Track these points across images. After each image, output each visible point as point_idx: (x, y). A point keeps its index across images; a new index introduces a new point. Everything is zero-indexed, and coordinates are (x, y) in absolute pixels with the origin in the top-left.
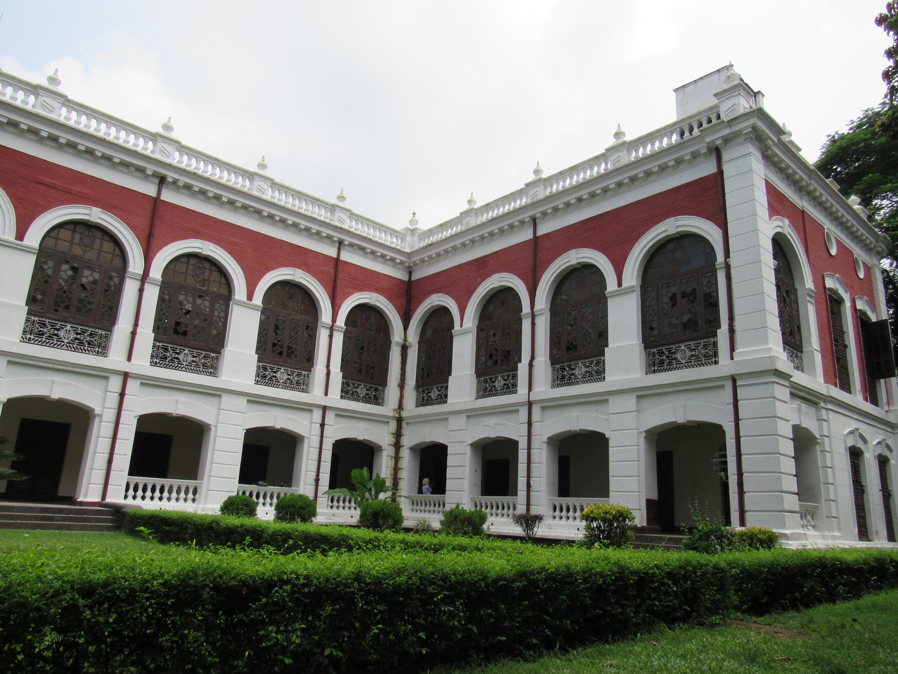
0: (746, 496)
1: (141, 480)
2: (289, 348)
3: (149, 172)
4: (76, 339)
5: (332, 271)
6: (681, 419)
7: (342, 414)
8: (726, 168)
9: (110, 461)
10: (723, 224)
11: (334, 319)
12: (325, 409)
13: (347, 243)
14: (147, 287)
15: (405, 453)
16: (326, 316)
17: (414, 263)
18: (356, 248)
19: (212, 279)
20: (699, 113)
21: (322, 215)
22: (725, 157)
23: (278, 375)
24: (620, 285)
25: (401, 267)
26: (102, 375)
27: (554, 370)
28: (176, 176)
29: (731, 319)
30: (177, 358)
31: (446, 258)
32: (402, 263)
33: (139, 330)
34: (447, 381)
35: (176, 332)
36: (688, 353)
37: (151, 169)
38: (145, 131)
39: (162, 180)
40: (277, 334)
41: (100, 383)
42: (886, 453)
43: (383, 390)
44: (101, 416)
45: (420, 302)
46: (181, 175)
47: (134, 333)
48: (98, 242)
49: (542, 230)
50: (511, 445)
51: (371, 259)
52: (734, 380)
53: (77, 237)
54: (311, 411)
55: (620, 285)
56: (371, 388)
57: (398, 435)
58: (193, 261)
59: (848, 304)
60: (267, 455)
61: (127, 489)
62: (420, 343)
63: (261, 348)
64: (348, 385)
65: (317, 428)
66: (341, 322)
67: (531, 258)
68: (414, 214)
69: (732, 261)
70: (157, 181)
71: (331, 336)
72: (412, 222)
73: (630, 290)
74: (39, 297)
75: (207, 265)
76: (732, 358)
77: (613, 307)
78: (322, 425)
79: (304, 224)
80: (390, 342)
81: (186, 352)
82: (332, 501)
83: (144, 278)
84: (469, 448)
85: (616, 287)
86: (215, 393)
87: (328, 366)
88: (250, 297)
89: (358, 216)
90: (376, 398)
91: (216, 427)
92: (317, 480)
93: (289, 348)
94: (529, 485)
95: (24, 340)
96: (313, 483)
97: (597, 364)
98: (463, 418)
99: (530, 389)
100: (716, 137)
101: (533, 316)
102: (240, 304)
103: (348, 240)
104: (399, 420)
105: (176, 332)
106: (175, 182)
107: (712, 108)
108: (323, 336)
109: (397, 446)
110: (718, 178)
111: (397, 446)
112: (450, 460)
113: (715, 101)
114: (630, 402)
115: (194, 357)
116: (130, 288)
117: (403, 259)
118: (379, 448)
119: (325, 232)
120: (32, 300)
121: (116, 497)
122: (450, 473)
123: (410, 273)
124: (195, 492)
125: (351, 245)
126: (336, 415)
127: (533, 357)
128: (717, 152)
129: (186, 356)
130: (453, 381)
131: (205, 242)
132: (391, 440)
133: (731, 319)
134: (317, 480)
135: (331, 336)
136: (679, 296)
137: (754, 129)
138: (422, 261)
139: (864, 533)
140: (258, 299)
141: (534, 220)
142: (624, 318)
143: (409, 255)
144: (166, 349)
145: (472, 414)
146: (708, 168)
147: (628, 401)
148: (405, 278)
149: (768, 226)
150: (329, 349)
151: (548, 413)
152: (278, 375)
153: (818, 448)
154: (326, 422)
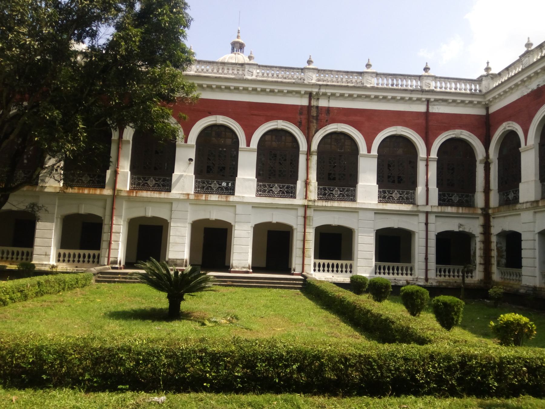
1: (322, 261)
2: (399, 177)
3: (303, 93)
4: (281, 191)
5: (424, 122)
9: (304, 253)
11: (428, 153)
12: (427, 213)
13: (432, 100)
15: (494, 239)
16: (422, 152)
17: (489, 100)
18: (441, 102)
19: (346, 143)
21: (413, 84)
23: (393, 195)
25: (480, 106)
28: (317, 90)
30: (332, 193)
31: (512, 93)
32: (479, 103)
34: (518, 187)
35: (329, 179)
37: (303, 90)
38: (298, 69)
39: (310, 95)
40: (390, 170)
41: (293, 212)
43: (473, 196)
44: (296, 229)
45: (496, 129)
48: (283, 138)
51: (455, 106)
53: (274, 137)
54: (418, 215)
56: (462, 195)
57: (487, 227)
58: (334, 136)
60: (393, 246)
62: (499, 159)
63: (380, 181)
64: (444, 195)
65: (423, 226)
66: (434, 155)
68: (488, 63)
70: (308, 96)
71: (427, 166)
72: (487, 69)
74: (261, 172)
75: (342, 137)
78: (427, 224)
79: (399, 95)
80: (476, 161)
81: (336, 189)
82: (440, 272)
84: (537, 236)
86: (355, 211)
87: (427, 185)
88: (369, 151)
89: (441, 78)
92: (426, 259)
93: (399, 177)
96: (424, 260)
102: (364, 156)
103: (432, 97)
105: (329, 179)
106: (317, 94)
108: (421, 166)
112: (524, 245)
115: (341, 191)
116: (302, 159)
117: (480, 100)
119: (415, 96)
120: (258, 175)
122: (524, 253)
124: (351, 267)
125: (436, 100)
126: (436, 216)
129: (336, 192)
130: (522, 186)
131: (339, 124)
134: (426, 259)
135: (427, 166)
138: (495, 98)
140: (374, 151)
143: (484, 95)
144: (325, 189)
148: (482, 112)
150: (427, 175)
152: (393, 195)
154: (429, 222)
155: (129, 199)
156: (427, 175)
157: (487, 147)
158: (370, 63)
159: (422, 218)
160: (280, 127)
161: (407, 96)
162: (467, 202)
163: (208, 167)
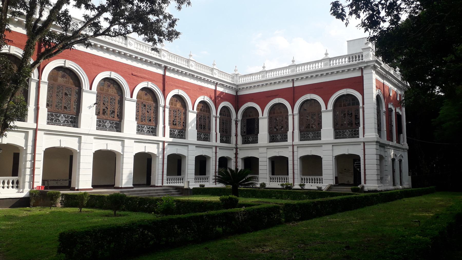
0: (366, 176)
1: (171, 177)
6: (347, 153)
7: (221, 148)
8: (364, 76)
10: (362, 94)
11: (217, 114)
12: (216, 147)
14: (166, 109)
17: (240, 89)
20: (356, 54)
22: (365, 72)
24: (326, 109)
26: (157, 142)
27: (301, 134)
29: (364, 124)
33: (166, 125)
36: (349, 133)
37: (163, 65)
39: (166, 68)
42: (402, 158)
46: (172, 65)
47: (164, 127)
49: (297, 84)
50: (285, 160)
52: (364, 143)
55: (326, 109)
57: (236, 154)
59: (394, 111)
61: (167, 180)
65: (214, 154)
67: (292, 94)
69: (365, 106)
71: (216, 120)
73: (329, 111)
76: (364, 137)
77: (324, 115)
78: (216, 153)
83: (164, 107)
85: (325, 109)
86: (186, 145)
87: (216, 131)
88: (193, 109)
90: (228, 141)
91: (188, 157)
94: (293, 172)
95: (137, 133)
97: (317, 133)
98: (266, 148)
99: (293, 141)
100: (362, 66)
101: (293, 116)
104: (237, 148)
105: (173, 124)
107: (360, 53)
109: (236, 158)
110: (361, 78)
111: (236, 158)
113: (361, 51)
114: (330, 147)
118: (230, 159)
119: (213, 80)
121: (165, 184)
123: (237, 92)
127: (293, 130)
128: (362, 70)
132: (234, 156)
133: (364, 124)
135: (216, 120)
136: (346, 115)
137: (374, 65)
138: (243, 88)
139: (394, 185)
141: (293, 80)
142: (327, 120)
143: (237, 86)
145: (268, 148)
146: (358, 74)
147: (328, 146)
149: (375, 92)
151: (299, 149)
153: (384, 160)
155: (48, 132)
156: (215, 125)
157: (237, 112)
158: (191, 54)
159: (214, 148)
160: (149, 86)
161: (210, 79)
162: (228, 141)
163: (104, 110)
